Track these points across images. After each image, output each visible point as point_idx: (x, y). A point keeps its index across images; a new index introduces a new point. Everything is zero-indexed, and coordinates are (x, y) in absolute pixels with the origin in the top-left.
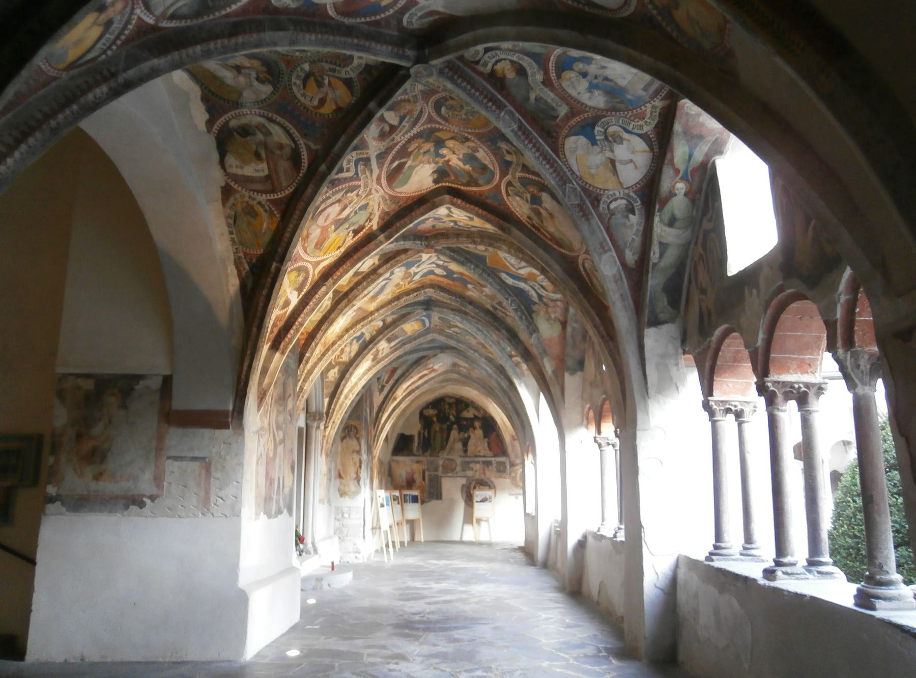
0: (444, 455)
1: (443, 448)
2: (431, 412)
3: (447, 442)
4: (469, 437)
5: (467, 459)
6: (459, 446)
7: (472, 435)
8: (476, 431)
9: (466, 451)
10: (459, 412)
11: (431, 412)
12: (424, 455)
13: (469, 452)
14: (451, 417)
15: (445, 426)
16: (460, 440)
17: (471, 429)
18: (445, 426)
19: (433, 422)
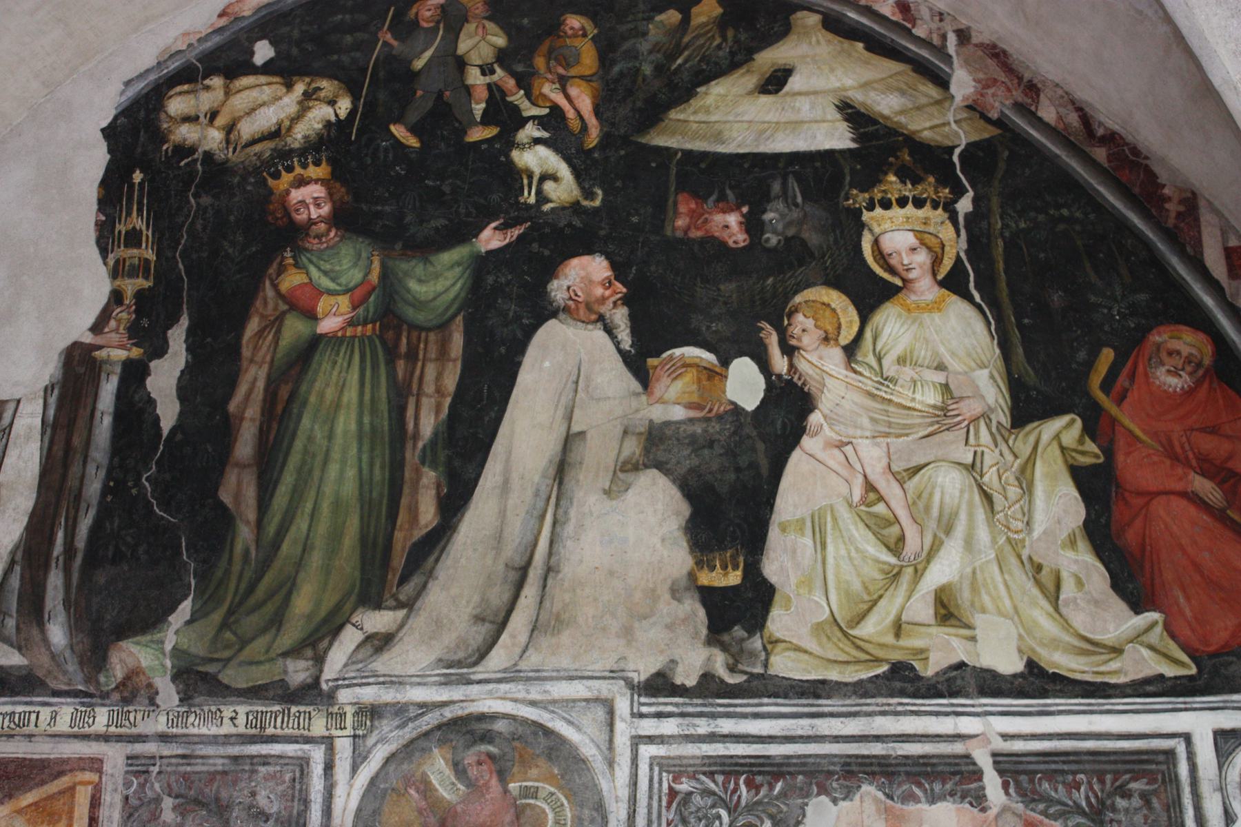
0: (406, 664)
1: (391, 567)
2: (269, 107)
3: (455, 501)
4: (790, 405)
5: (765, 729)
6: (638, 532)
7: (821, 365)
8: (892, 327)
9: (738, 610)
10: (643, 96)
11: (269, 107)
12: (91, 674)
13: (797, 635)
14: (535, 158)
15: (437, 281)
16: (656, 447)
17: (821, 308)
18: (437, 281)
19: (289, 235)
